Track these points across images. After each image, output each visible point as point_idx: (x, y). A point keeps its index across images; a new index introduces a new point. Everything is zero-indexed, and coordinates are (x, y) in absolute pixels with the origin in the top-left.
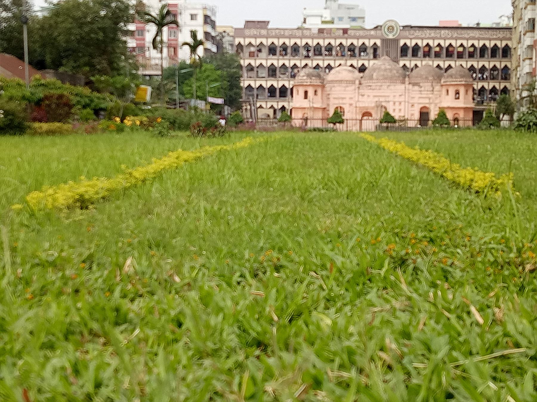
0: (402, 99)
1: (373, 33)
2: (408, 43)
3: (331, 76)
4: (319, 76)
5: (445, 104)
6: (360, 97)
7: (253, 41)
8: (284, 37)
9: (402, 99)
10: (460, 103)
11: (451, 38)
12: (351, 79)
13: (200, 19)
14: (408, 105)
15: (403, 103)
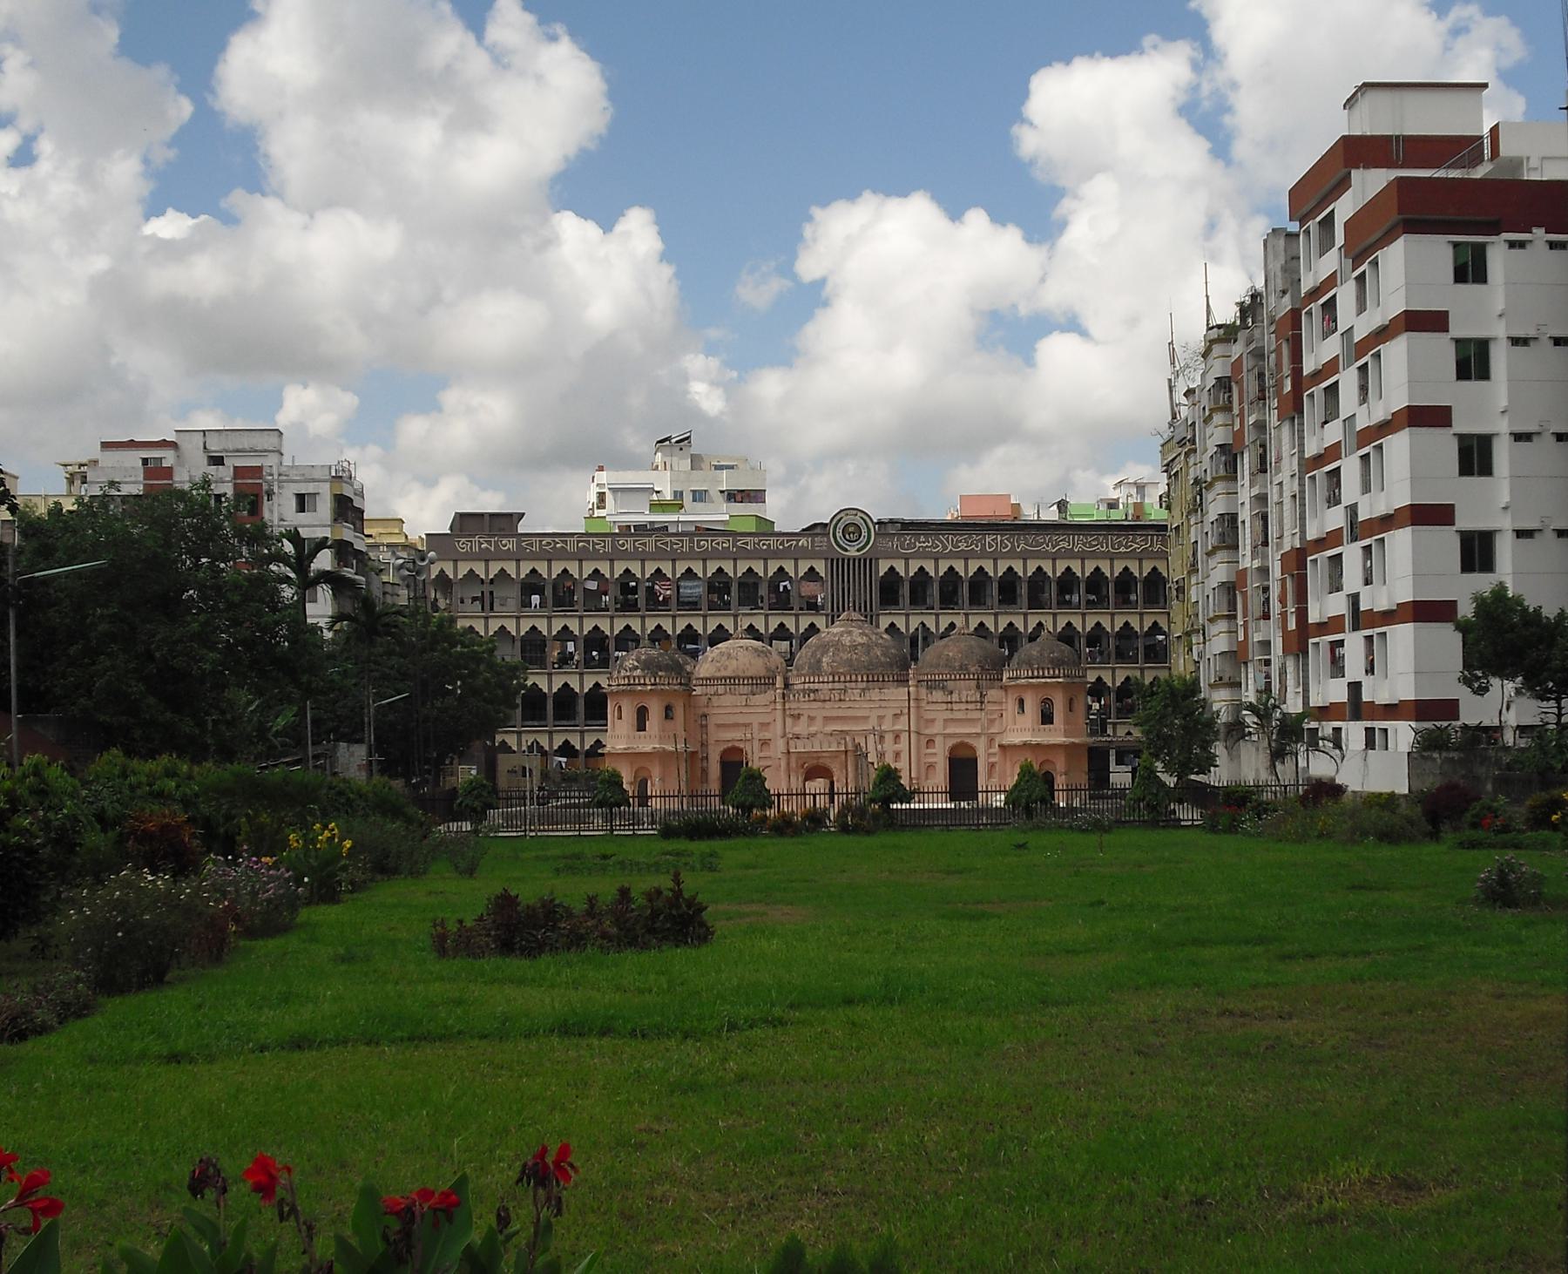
0: (901, 725)
1: (803, 542)
2: (900, 567)
3: (709, 663)
4: (677, 669)
5: (1016, 739)
6: (789, 721)
7: (479, 569)
8: (563, 555)
9: (901, 725)
10: (1055, 735)
11: (1012, 554)
12: (763, 673)
13: (325, 508)
14: (918, 741)
15: (904, 736)
